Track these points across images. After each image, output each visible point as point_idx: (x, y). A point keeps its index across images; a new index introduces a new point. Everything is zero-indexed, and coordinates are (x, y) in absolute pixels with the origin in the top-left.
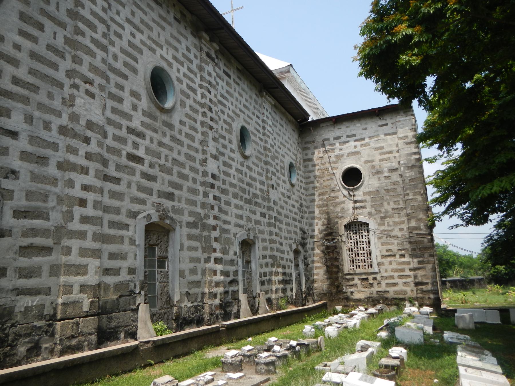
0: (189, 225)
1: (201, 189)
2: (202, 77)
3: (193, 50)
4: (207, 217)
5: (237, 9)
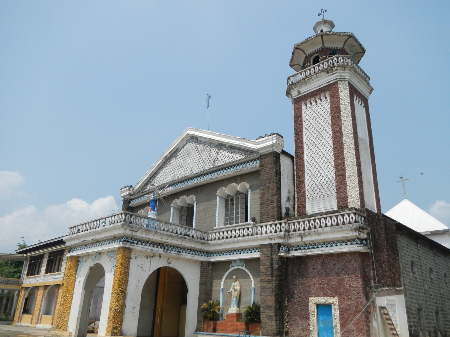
0: (441, 310)
1: (440, 299)
2: (435, 263)
3: (432, 255)
4: (443, 307)
5: (405, 180)
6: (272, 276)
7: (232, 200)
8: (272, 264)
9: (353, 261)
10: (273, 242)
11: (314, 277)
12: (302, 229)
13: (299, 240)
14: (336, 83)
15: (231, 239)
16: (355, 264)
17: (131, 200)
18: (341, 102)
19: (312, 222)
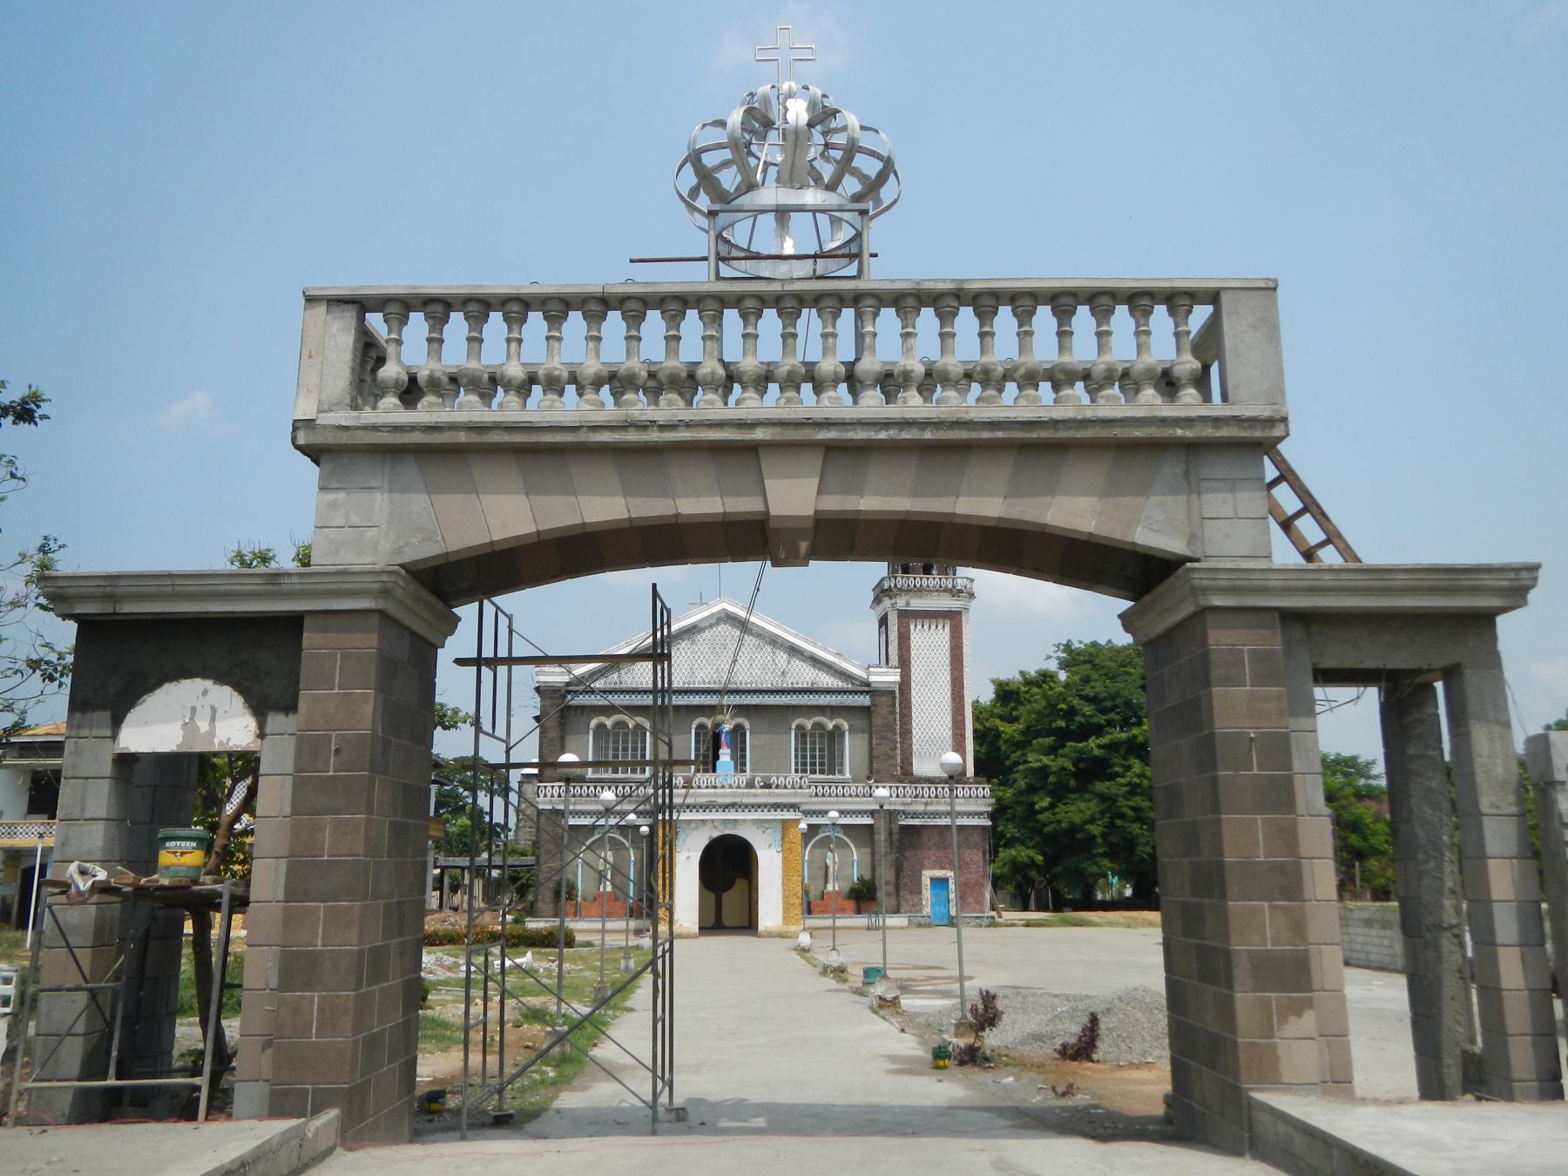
6: (891, 848)
7: (804, 736)
8: (891, 834)
9: (976, 835)
10: (892, 808)
11: (930, 849)
12: (926, 796)
13: (921, 808)
14: (959, 613)
15: (842, 799)
16: (977, 838)
17: (569, 692)
18: (964, 641)
19: (940, 789)
